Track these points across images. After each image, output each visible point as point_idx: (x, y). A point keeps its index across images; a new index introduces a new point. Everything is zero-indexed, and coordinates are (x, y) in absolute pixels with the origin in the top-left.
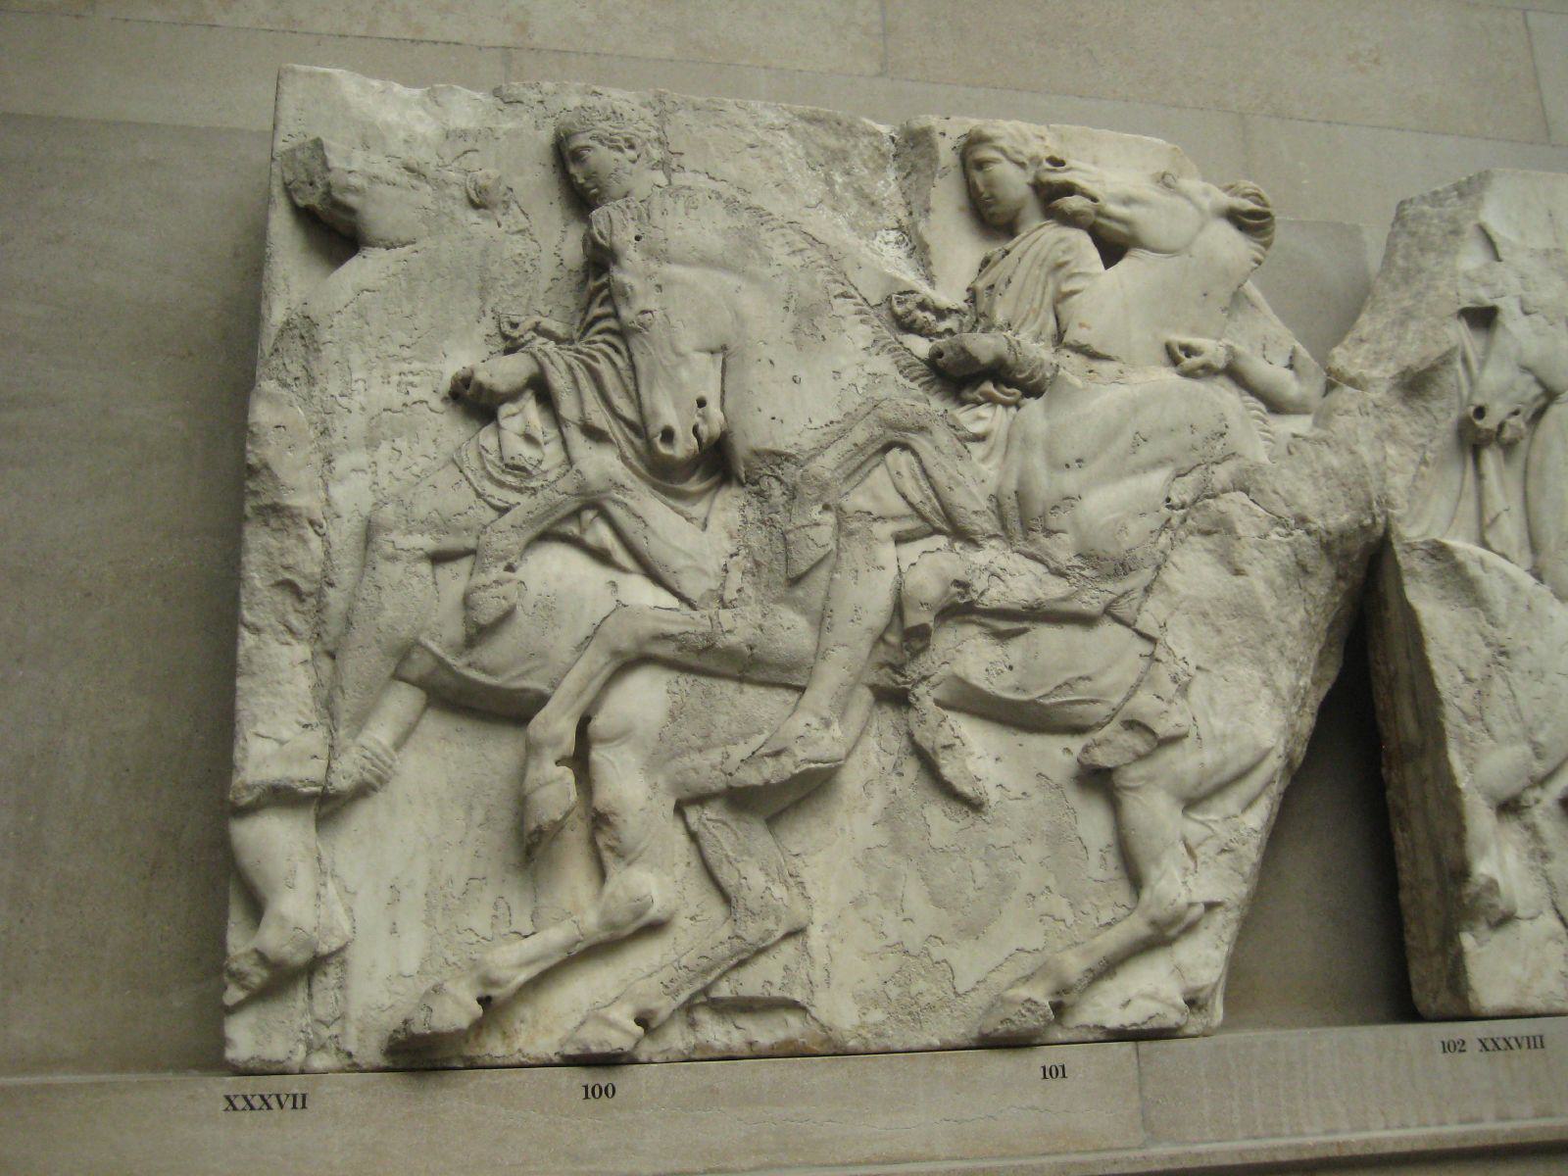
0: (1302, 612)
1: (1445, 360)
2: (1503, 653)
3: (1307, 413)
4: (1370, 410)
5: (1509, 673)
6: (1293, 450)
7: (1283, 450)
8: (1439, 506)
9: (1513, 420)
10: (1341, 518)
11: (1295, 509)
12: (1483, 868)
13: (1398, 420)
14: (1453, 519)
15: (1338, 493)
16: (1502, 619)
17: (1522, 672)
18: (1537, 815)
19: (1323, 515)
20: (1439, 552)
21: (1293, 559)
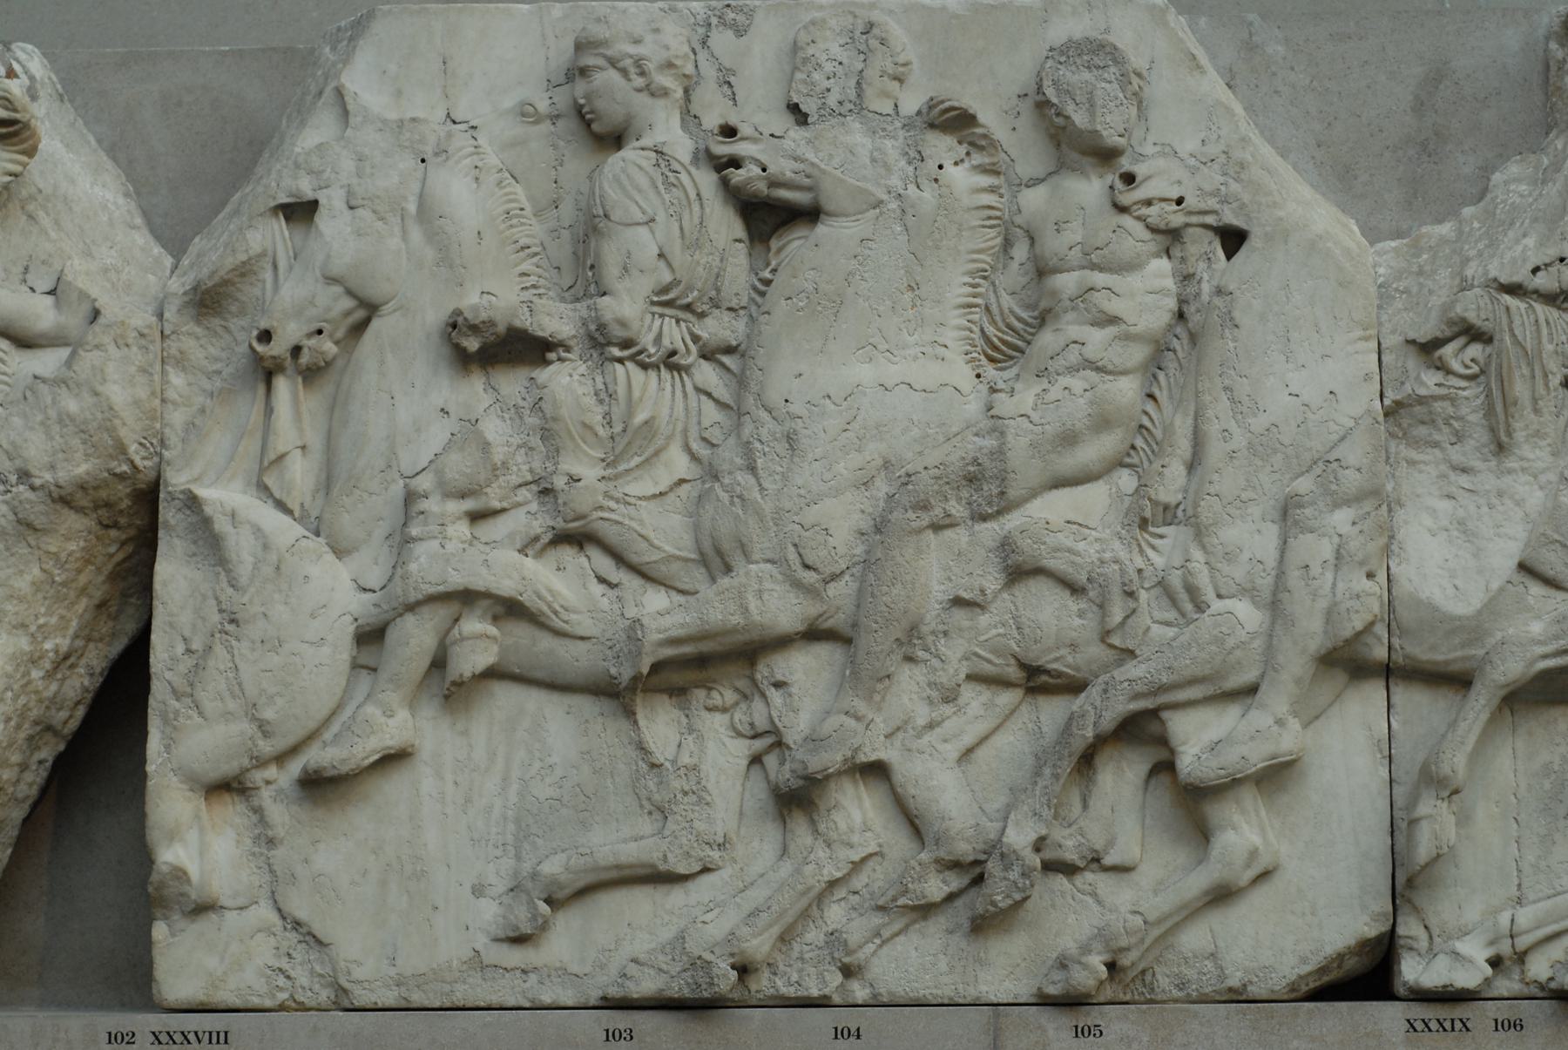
0: (36, 571)
1: (245, 271)
2: (232, 621)
3: (67, 345)
4: (130, 341)
5: (234, 643)
6: (28, 394)
7: (20, 395)
8: (217, 444)
9: (313, 342)
10: (82, 468)
11: (18, 463)
12: (169, 855)
13: (189, 344)
14: (232, 458)
15: (76, 442)
16: (243, 581)
17: (253, 642)
18: (266, 796)
19: (52, 467)
20: (192, 502)
21: (11, 517)
